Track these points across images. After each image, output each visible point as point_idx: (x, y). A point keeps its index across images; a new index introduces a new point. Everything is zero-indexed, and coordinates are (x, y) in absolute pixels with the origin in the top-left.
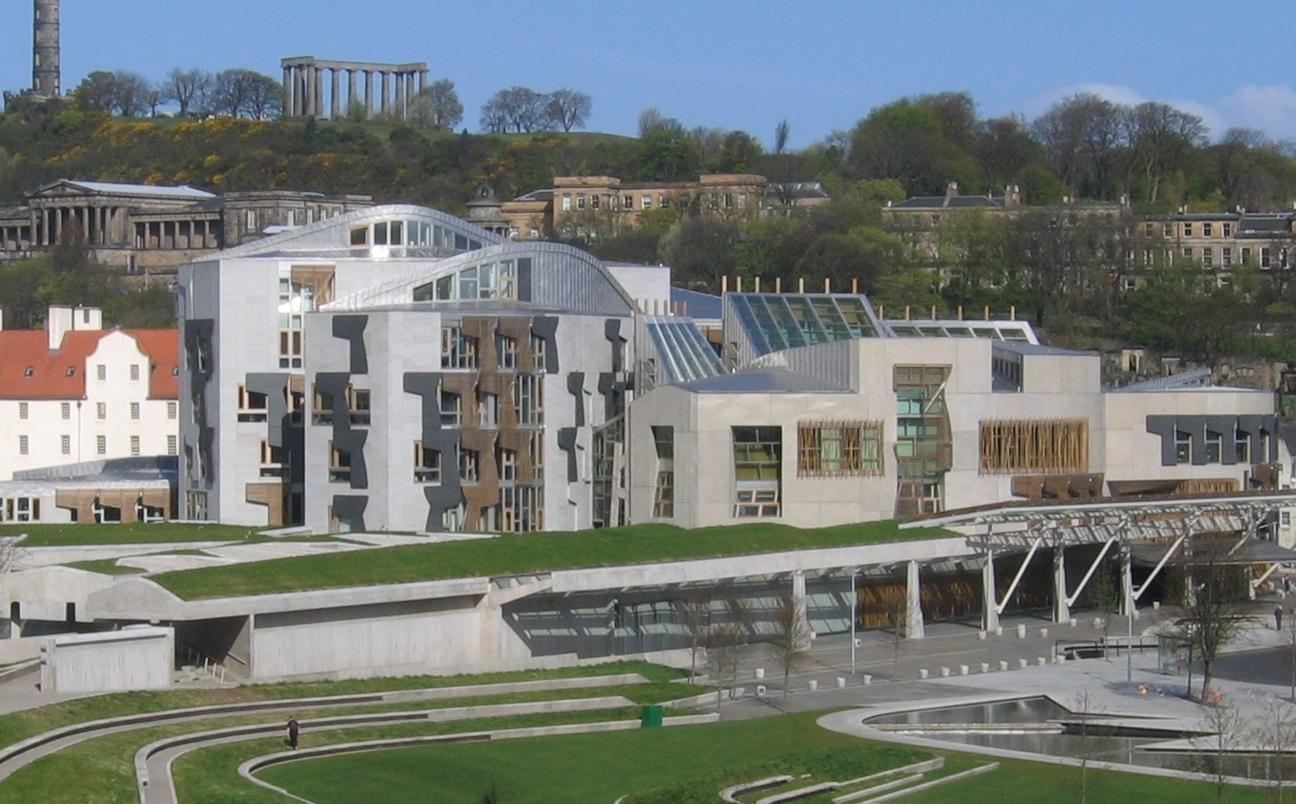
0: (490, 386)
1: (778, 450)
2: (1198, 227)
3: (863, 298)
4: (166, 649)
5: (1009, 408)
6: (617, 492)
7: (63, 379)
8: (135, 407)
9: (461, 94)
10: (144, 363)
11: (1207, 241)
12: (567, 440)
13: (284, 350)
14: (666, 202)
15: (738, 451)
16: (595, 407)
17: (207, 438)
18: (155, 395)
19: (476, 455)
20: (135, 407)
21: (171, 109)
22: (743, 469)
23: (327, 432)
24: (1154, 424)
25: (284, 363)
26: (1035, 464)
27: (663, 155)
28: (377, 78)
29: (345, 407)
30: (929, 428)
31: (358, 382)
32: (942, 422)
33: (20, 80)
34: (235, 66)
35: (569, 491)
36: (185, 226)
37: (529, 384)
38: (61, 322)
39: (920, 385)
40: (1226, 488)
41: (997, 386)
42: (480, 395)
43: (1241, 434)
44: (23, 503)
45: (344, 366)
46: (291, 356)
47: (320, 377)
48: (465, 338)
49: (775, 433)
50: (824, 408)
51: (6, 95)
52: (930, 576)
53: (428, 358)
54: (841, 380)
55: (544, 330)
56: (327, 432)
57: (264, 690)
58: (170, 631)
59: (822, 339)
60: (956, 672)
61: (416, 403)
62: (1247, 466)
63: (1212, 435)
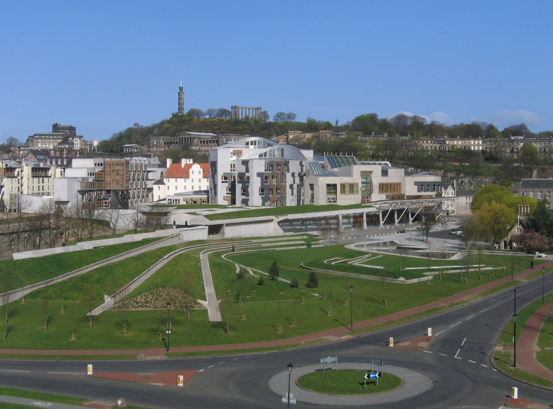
0: (275, 175)
1: (336, 189)
2: (425, 141)
3: (354, 157)
4: (206, 231)
5: (385, 180)
6: (302, 198)
7: (185, 174)
8: (200, 180)
9: (269, 114)
10: (202, 170)
11: (427, 145)
12: (291, 187)
13: (231, 168)
14: (312, 136)
15: (327, 189)
16: (297, 180)
17: (215, 186)
18: (203, 178)
19: (272, 190)
20: (200, 180)
21: (207, 117)
22: (329, 193)
23: (241, 185)
24: (416, 183)
25: (231, 170)
26: (391, 192)
27: (311, 126)
28: (251, 110)
29: (244, 180)
30: (368, 184)
31: (247, 174)
32: (371, 183)
33: (176, 111)
34: (221, 108)
35: (292, 197)
36: (210, 141)
37: (283, 175)
38: (184, 162)
39: (366, 175)
40: (431, 197)
41: (382, 175)
42: (273, 177)
43: (434, 185)
44: (176, 200)
45: (244, 171)
46: (233, 169)
47: (239, 173)
48: (270, 165)
49: (335, 185)
50: (346, 180)
51: (172, 114)
52: (368, 216)
53: (262, 170)
54: (349, 174)
55: (286, 164)
56: (241, 185)
57: (227, 240)
58: (207, 227)
59: (345, 165)
60: (374, 236)
61: (259, 179)
62: (435, 192)
63: (428, 186)
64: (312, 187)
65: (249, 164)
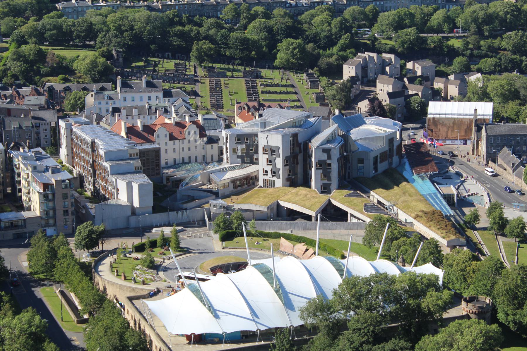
6: (348, 171)
8: (166, 143)
20: (166, 143)
31: (329, 162)
47: (318, 160)
56: (321, 171)
64: (361, 161)
65: (332, 153)
